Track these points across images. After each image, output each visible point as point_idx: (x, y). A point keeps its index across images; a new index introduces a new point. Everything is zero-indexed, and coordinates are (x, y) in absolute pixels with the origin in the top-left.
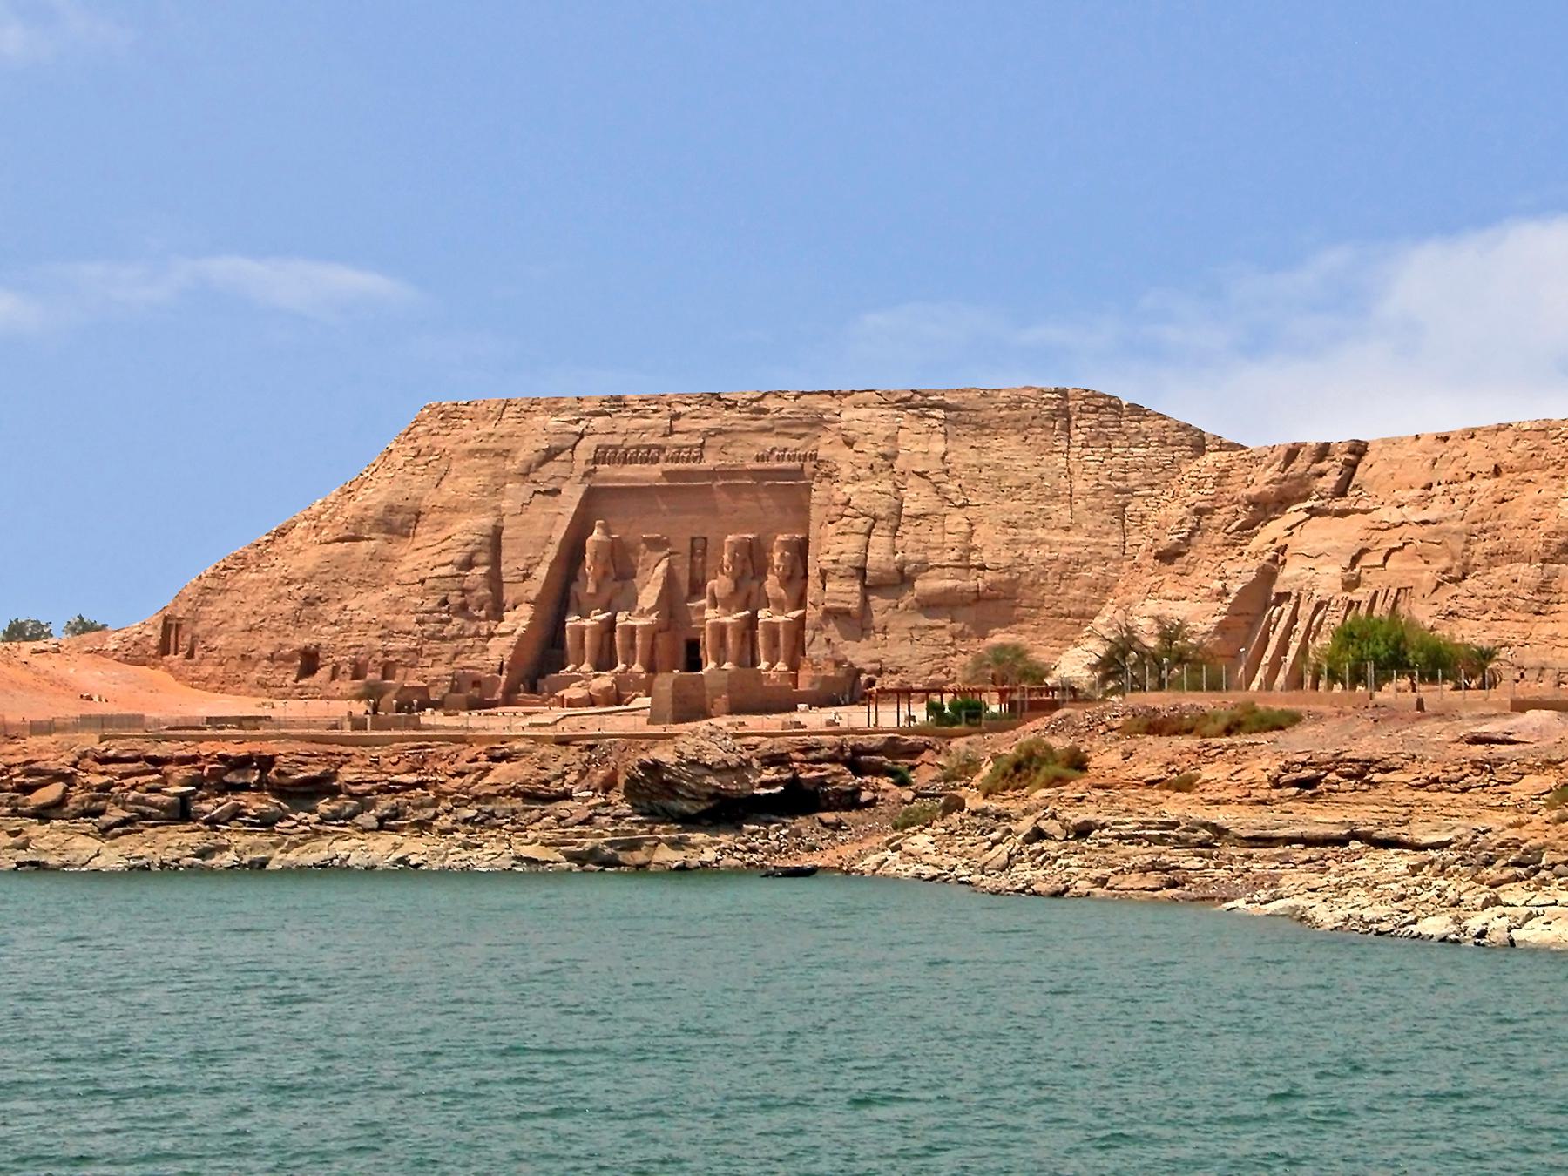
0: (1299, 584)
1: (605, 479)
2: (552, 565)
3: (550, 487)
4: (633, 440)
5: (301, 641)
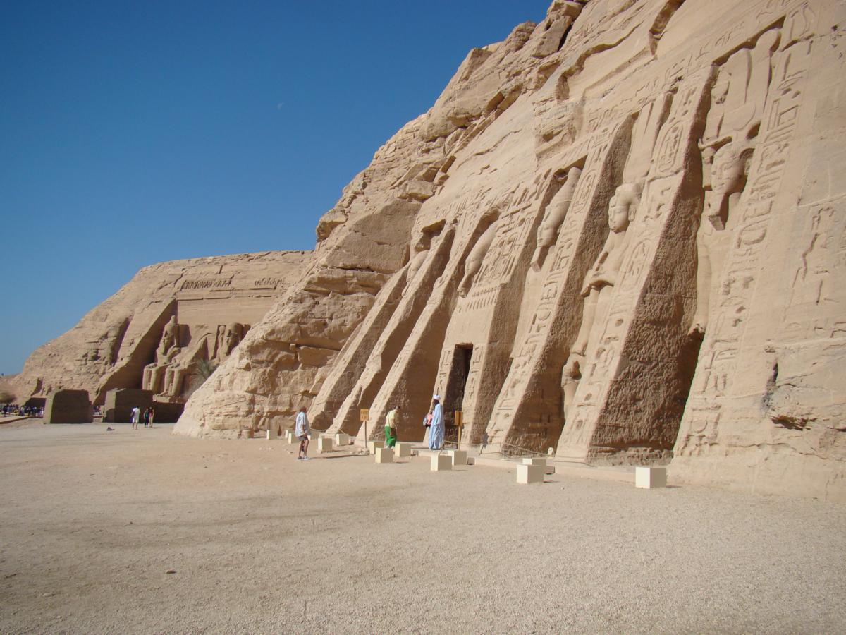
0: (459, 201)
1: (183, 296)
2: (144, 338)
3: (159, 299)
4: (202, 278)
5: (40, 375)
